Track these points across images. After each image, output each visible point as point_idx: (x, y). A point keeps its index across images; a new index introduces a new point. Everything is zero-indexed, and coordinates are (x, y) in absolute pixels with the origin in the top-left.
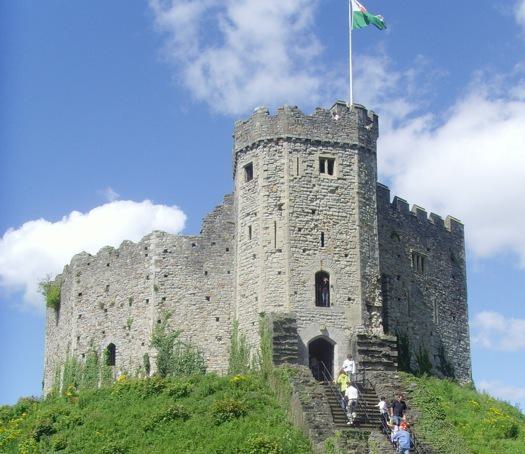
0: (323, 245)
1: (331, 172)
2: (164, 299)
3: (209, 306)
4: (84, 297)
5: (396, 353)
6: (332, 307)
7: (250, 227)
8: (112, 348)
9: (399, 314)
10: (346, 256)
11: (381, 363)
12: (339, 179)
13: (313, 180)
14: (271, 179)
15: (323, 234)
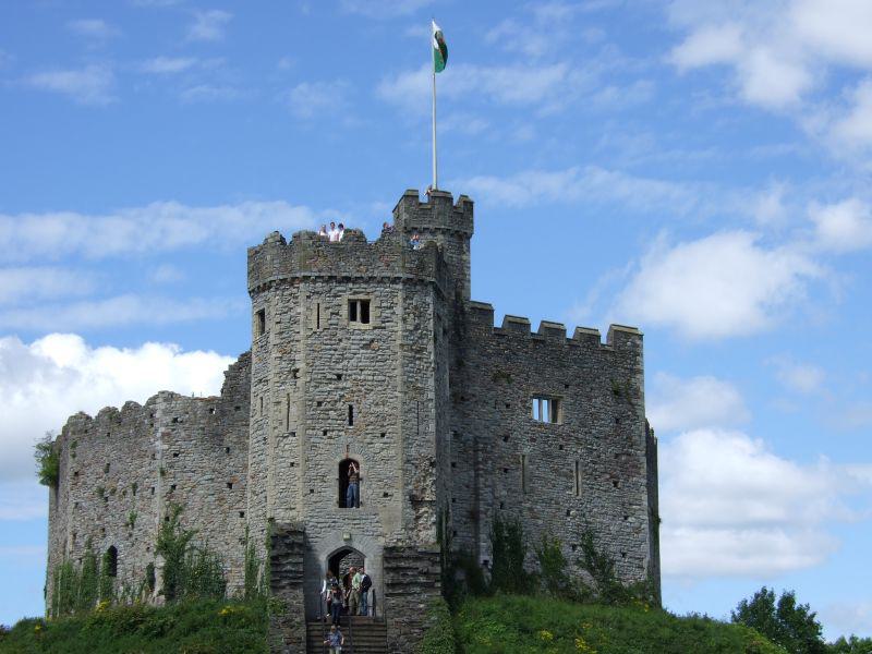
0: (351, 423)
1: (365, 319)
2: (174, 487)
3: (231, 497)
4: (82, 479)
5: (438, 569)
6: (361, 508)
7: (262, 399)
8: (113, 551)
9: (504, 493)
10: (383, 435)
11: (417, 584)
12: (375, 328)
13: (340, 334)
14: (284, 335)
15: (351, 408)
